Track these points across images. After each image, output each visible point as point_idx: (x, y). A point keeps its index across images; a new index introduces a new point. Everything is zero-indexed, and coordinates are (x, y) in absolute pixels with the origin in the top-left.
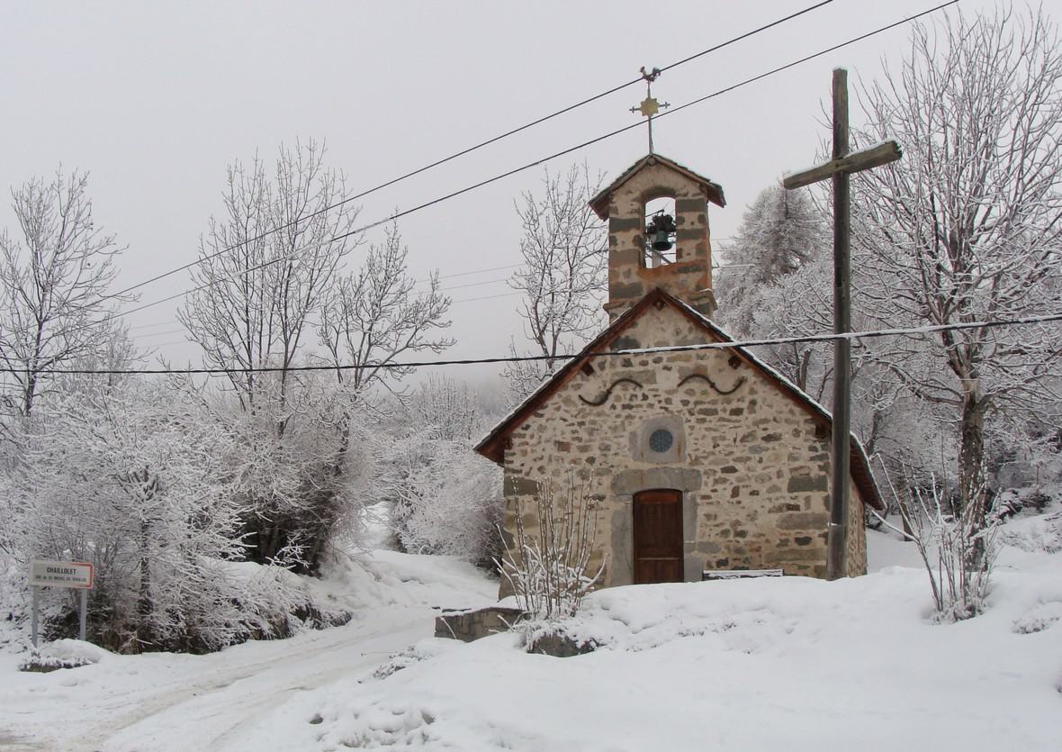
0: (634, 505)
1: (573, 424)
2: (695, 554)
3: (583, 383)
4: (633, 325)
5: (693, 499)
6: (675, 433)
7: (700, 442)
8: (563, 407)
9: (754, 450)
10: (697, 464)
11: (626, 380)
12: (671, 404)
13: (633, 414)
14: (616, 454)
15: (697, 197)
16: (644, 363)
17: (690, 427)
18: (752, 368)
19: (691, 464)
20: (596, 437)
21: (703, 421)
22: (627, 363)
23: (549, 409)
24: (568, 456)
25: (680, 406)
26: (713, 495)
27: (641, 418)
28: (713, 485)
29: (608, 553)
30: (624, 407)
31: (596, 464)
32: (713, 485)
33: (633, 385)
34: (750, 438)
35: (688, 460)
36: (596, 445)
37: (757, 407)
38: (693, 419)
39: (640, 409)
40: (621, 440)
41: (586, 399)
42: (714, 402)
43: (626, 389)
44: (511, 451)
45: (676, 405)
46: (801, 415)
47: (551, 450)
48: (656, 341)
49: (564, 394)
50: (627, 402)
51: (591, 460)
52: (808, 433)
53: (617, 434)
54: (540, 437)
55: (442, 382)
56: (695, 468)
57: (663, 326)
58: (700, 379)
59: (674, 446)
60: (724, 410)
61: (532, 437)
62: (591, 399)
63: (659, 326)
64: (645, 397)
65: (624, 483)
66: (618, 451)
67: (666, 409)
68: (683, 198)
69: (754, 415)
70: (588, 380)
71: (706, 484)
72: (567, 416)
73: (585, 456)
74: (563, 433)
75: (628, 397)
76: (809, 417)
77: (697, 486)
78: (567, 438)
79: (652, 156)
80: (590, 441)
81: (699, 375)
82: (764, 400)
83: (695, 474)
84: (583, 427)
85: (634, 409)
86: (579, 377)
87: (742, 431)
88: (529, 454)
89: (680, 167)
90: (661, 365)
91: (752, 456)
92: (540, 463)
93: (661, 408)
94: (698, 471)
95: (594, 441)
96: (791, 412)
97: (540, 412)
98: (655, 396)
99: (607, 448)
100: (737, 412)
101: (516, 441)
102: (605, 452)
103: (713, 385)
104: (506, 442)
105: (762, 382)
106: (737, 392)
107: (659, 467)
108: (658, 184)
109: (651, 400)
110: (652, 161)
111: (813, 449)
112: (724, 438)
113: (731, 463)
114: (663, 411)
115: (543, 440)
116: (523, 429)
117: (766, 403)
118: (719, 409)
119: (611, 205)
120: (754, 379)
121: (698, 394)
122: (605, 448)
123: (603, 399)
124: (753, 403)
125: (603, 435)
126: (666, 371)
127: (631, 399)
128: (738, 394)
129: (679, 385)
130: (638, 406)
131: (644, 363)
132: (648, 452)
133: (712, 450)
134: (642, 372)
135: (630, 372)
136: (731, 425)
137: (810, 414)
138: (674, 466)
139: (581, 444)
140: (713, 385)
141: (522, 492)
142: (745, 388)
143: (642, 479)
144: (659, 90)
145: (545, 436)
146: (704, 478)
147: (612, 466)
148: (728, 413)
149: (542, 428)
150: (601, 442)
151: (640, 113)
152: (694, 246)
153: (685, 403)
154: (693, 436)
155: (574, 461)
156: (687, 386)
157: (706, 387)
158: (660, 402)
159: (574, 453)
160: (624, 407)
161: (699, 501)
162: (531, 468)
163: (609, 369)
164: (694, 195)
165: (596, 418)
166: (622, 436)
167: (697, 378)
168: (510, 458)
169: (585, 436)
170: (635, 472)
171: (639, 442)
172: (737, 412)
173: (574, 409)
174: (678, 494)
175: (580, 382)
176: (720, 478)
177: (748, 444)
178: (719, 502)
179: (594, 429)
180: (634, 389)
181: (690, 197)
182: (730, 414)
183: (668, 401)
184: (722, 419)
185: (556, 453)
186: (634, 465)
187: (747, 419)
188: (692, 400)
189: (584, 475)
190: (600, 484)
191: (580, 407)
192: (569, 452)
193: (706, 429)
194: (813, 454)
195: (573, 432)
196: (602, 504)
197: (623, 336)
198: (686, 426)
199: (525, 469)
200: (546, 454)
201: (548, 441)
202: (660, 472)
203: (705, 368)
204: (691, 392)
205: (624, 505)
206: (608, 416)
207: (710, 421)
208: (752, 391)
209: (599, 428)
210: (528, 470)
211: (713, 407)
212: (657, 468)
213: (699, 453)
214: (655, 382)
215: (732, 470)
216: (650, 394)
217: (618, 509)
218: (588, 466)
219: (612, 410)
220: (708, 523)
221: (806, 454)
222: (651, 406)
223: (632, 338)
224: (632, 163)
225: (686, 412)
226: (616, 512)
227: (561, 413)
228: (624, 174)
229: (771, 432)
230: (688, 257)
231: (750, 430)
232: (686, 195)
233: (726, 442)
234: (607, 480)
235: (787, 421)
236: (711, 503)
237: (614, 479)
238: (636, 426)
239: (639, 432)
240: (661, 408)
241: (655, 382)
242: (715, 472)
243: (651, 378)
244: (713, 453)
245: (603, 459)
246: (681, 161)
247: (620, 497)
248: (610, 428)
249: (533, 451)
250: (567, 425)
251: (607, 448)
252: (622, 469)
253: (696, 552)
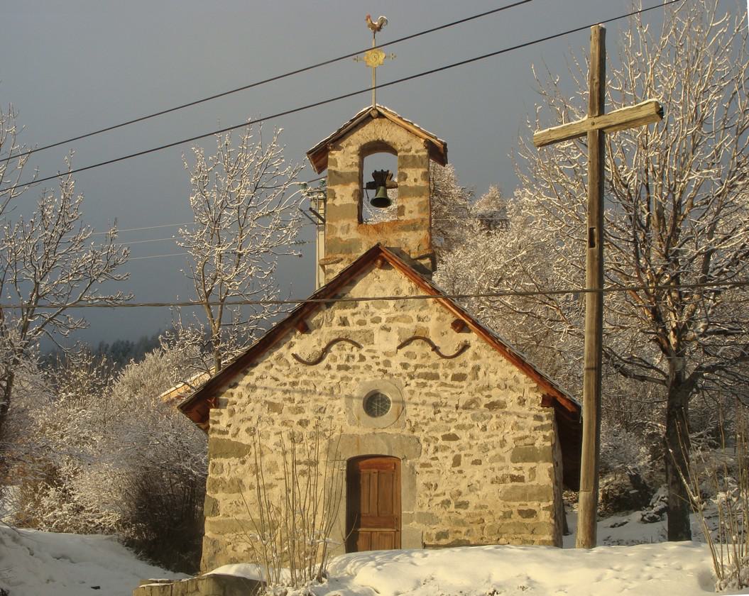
5: (412, 467)
13: (350, 376)
25: (400, 370)
26: (433, 463)
27: (357, 380)
30: (340, 368)
33: (350, 345)
38: (413, 383)
42: (435, 366)
51: (303, 423)
76: (535, 385)
92: (248, 424)
93: (379, 370)
100: (459, 377)
102: (319, 415)
103: (435, 349)
113: (453, 431)
124: (476, 369)
127: (348, 360)
130: (355, 367)
131: (361, 323)
141: (226, 455)
149: (253, 388)
153: (405, 366)
158: (378, 364)
161: (417, 468)
170: (352, 436)
172: (459, 377)
183: (387, 363)
184: (444, 384)
195: (285, 392)
202: (375, 436)
206: (325, 377)
211: (434, 371)
213: (419, 419)
215: (454, 438)
218: (299, 429)
219: (326, 371)
240: (379, 370)
243: (369, 337)
244: (433, 420)
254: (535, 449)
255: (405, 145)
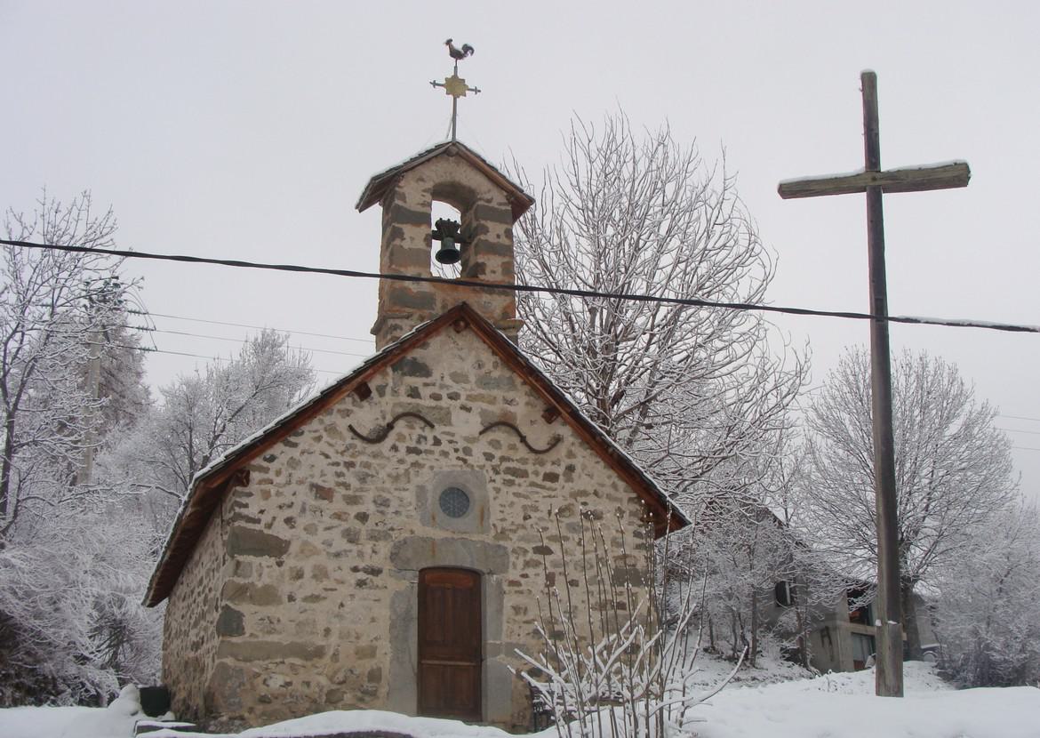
0: (419, 584)
1: (337, 464)
2: (501, 658)
3: (355, 409)
4: (424, 345)
5: (499, 584)
6: (476, 494)
7: (507, 510)
8: (326, 437)
9: (572, 528)
10: (502, 539)
11: (414, 415)
12: (471, 455)
13: (421, 461)
14: (397, 513)
15: (503, 208)
16: (437, 397)
17: (494, 488)
18: (572, 426)
19: (496, 537)
20: (369, 485)
21: (511, 483)
22: (414, 393)
23: (306, 436)
24: (330, 507)
25: (482, 461)
26: (523, 581)
27: (432, 468)
28: (523, 569)
29: (385, 647)
30: (410, 450)
31: (370, 523)
32: (523, 569)
33: (423, 424)
34: (567, 513)
35: (493, 533)
36: (369, 496)
37: (575, 475)
38: (498, 478)
39: (430, 456)
40: (404, 494)
41: (358, 430)
42: (524, 461)
43: (412, 427)
44: (246, 490)
45: (477, 459)
46: (625, 491)
47: (305, 496)
48: (452, 371)
49: (328, 420)
50: (413, 444)
51: (363, 517)
52: (632, 514)
53: (401, 485)
54: (290, 475)
55: (978, 408)
56: (501, 543)
57: (463, 354)
58: (508, 429)
59: (474, 511)
60: (536, 473)
61: (278, 473)
62: (364, 433)
63: (456, 352)
64: (437, 442)
65: (409, 553)
66: (400, 509)
67: (465, 461)
68: (486, 204)
69: (570, 484)
70: (361, 407)
71: (515, 565)
72: (330, 451)
73: (353, 510)
74: (323, 474)
75: (415, 437)
76: (634, 495)
77: (504, 568)
78: (330, 482)
79: (455, 143)
80: (361, 490)
81: (507, 423)
82: (584, 467)
83: (501, 552)
84: (352, 469)
85: (423, 455)
86: (349, 400)
87: (557, 504)
88: (273, 498)
89: (488, 165)
90: (458, 403)
91: (570, 535)
92: (288, 513)
93: (458, 458)
94: (505, 548)
95: (367, 490)
96: (614, 486)
97: (293, 439)
98: (451, 442)
99: (386, 503)
100: (552, 477)
101: (255, 476)
102: (382, 508)
103: (523, 439)
104: (244, 475)
105: (581, 444)
106: (551, 452)
107: (455, 536)
108: (457, 179)
109: (445, 446)
110: (454, 150)
111: (637, 534)
112: (536, 509)
113: (546, 543)
114: (461, 463)
115: (294, 480)
116: (265, 459)
117: (586, 472)
118: (530, 472)
119: (397, 189)
120: (571, 439)
121: (505, 448)
122: (383, 503)
123: (380, 436)
124: (571, 469)
125: (380, 485)
126: (463, 412)
127: (419, 442)
128: (553, 455)
129: (481, 433)
130: (427, 452)
131: (437, 397)
132: (441, 516)
133: (522, 522)
134: (434, 408)
135: (418, 404)
136: (545, 493)
137: (635, 492)
138: (475, 538)
139: (350, 493)
140: (523, 439)
141: (259, 552)
142: (562, 450)
143: (434, 551)
144: (466, 68)
145: (299, 474)
146: (512, 558)
147: (392, 529)
148: (541, 477)
149: (293, 463)
150: (378, 494)
151: (444, 90)
152: (500, 263)
153: (489, 457)
154: (499, 501)
155: (338, 516)
156: (491, 436)
157: (516, 440)
158: (456, 450)
159: (338, 504)
160: (410, 450)
161: (506, 587)
162: (274, 518)
163: (391, 395)
164: (500, 204)
165: (371, 460)
166: (405, 490)
167: (503, 428)
168: (244, 500)
169: (354, 483)
170: (424, 540)
171: (429, 495)
172: (552, 477)
173: (340, 442)
174: (474, 577)
175: (350, 407)
176: (532, 559)
177: (566, 520)
178: (530, 591)
179: (368, 475)
180: (423, 429)
181: (494, 204)
182: (544, 480)
183: (467, 451)
184: (533, 484)
185: (312, 501)
186: (421, 530)
187: (563, 488)
188: (498, 454)
189: (351, 537)
190: (374, 552)
191: (349, 441)
192: (331, 502)
193: (514, 494)
194: (639, 541)
195: (339, 475)
196: (377, 580)
197: (409, 356)
198: (490, 486)
199: (266, 518)
200: (298, 500)
201: (301, 482)
202: (458, 544)
203: (513, 416)
204: (495, 444)
205: (407, 585)
206: (387, 460)
207: (520, 485)
208: (571, 455)
209: (374, 473)
210: (270, 520)
211: (522, 467)
212: (453, 539)
213: (506, 525)
214: (450, 424)
215: (545, 551)
216: (444, 439)
217: (400, 588)
218: (357, 525)
219: (393, 453)
220: (517, 618)
221: (630, 540)
222: (445, 454)
223: (420, 361)
224: (431, 145)
225: (490, 469)
226: (397, 594)
227: (322, 446)
228: (421, 155)
229: (591, 507)
230: (493, 275)
231: (566, 503)
232: (489, 201)
233: (538, 515)
234: (384, 548)
235: (609, 496)
236: (521, 592)
237: (395, 547)
238: (425, 477)
239: (429, 487)
240: (458, 458)
241: (450, 424)
242: (526, 552)
243: (446, 418)
244: (524, 527)
245: (378, 517)
246: (493, 157)
247: (404, 572)
248: (389, 476)
249: (278, 494)
250: (329, 464)
251: (386, 503)
252: (407, 535)
253: (502, 656)
254: (636, 571)
255: (485, 193)
